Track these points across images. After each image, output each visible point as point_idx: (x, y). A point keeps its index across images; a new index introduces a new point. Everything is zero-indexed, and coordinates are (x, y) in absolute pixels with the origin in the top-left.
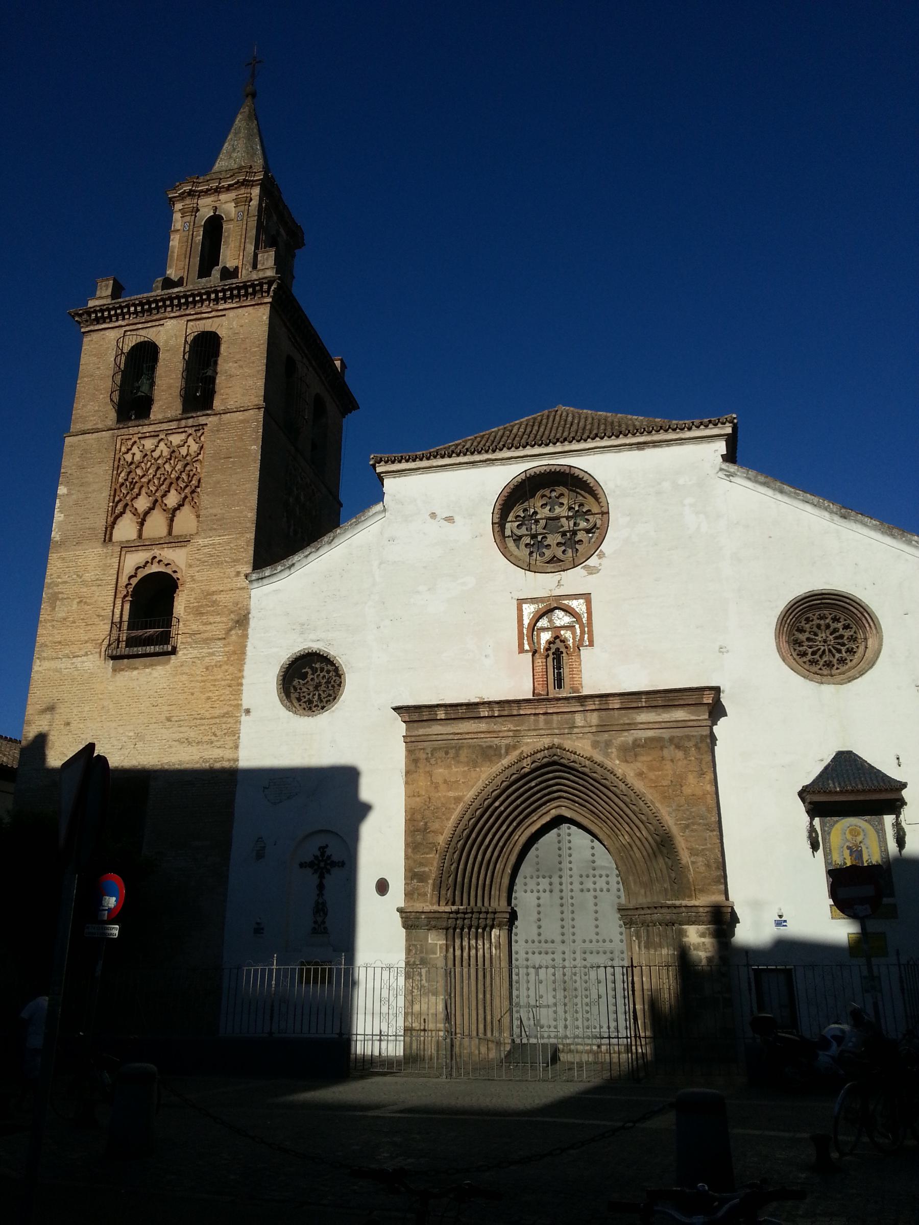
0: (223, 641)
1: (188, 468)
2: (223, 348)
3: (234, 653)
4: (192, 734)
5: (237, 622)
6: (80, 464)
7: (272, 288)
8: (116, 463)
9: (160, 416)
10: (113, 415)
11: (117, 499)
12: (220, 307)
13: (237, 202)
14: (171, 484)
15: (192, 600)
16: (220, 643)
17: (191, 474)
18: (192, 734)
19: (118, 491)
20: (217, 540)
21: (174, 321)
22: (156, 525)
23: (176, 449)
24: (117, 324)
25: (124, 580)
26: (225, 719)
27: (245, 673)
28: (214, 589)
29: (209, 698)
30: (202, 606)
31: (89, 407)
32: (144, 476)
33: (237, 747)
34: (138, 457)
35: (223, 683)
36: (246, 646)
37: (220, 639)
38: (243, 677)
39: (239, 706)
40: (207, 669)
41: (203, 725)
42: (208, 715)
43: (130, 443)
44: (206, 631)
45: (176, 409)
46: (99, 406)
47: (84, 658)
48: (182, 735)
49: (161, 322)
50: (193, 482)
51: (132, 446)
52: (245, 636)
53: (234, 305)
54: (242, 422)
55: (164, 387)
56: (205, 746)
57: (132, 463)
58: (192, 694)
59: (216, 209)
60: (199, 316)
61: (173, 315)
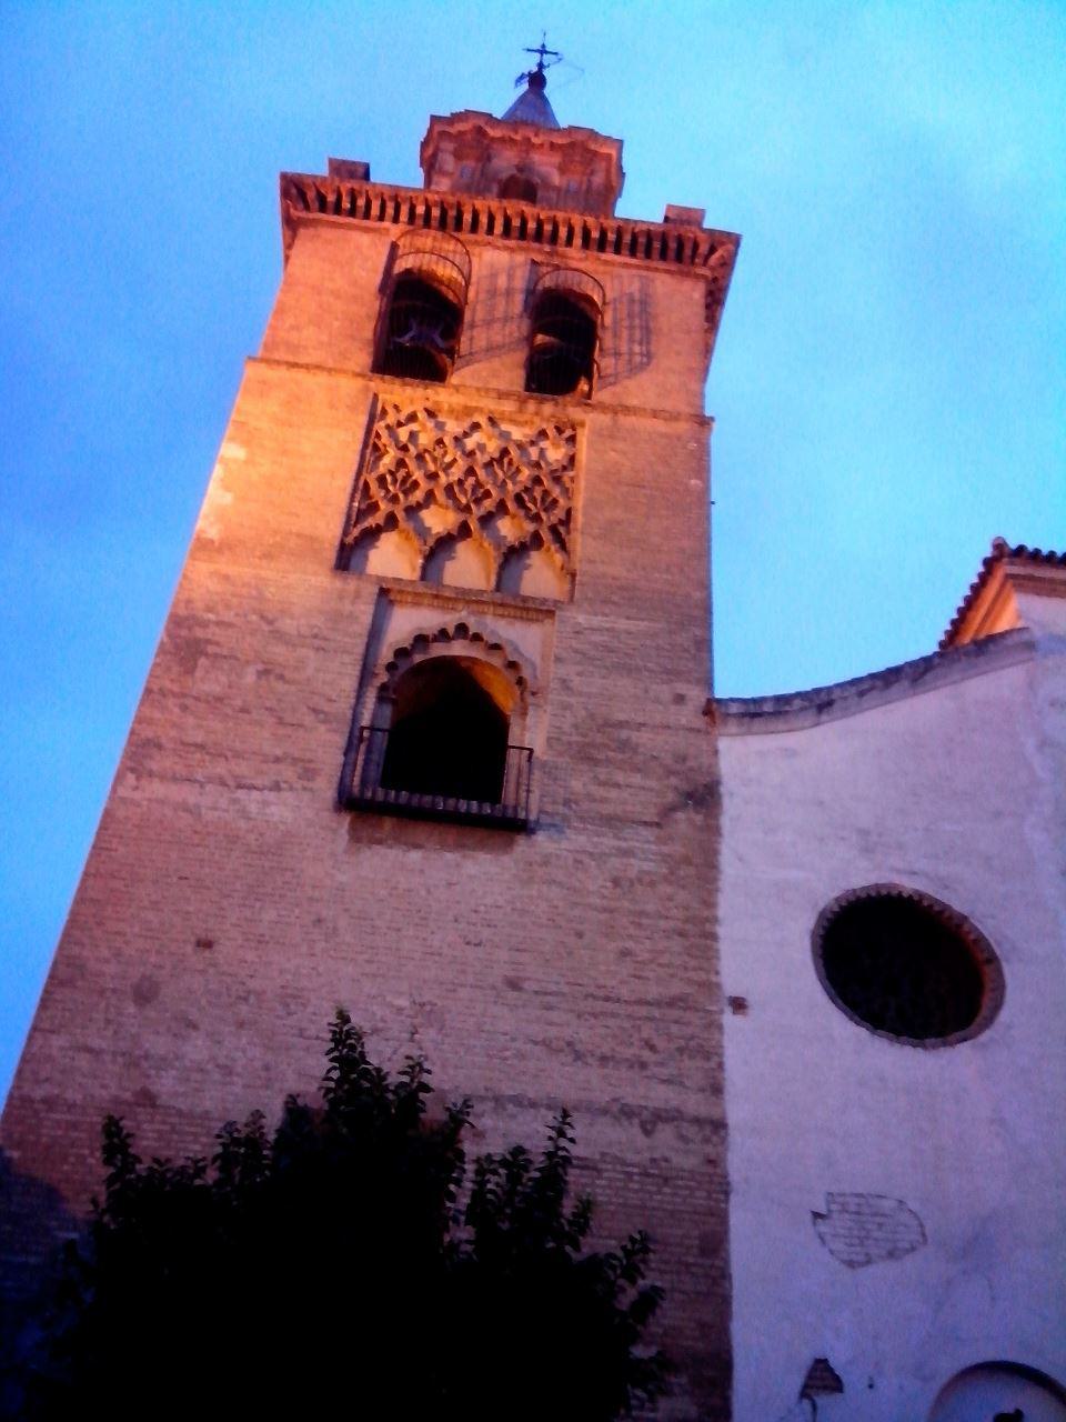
0: (656, 831)
3: (687, 861)
4: (584, 1034)
5: (690, 795)
15: (566, 728)
16: (646, 833)
18: (584, 1034)
20: (623, 624)
22: (468, 568)
25: (386, 655)
26: (675, 1013)
27: (722, 912)
28: (622, 717)
29: (625, 953)
30: (592, 745)
33: (717, 1089)
35: (662, 924)
36: (716, 853)
37: (645, 823)
38: (715, 920)
39: (711, 988)
40: (616, 882)
41: (614, 1015)
42: (624, 992)
44: (603, 800)
47: (271, 796)
48: (553, 1032)
52: (712, 830)
56: (624, 1072)
58: (580, 935)
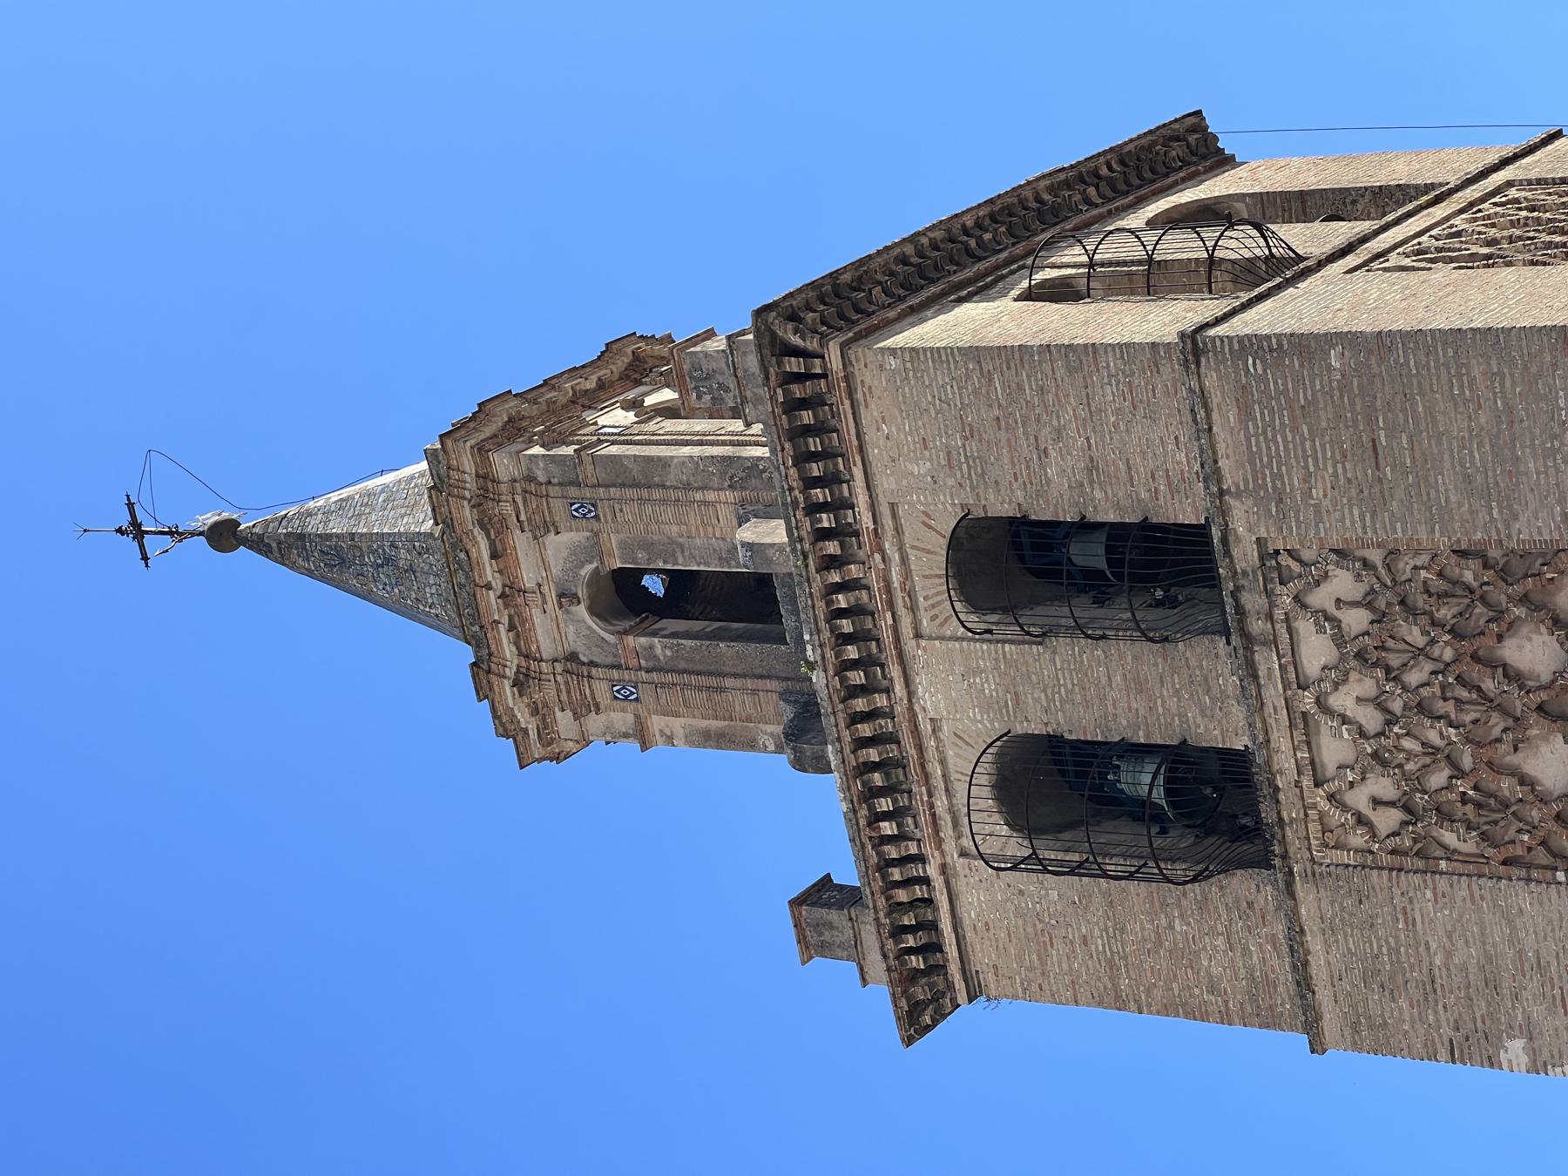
1: (1420, 601)
2: (1001, 506)
6: (1417, 995)
7: (796, 340)
8: (1408, 862)
9: (1238, 714)
10: (1241, 884)
11: (1541, 856)
12: (866, 521)
13: (543, 527)
14: (1475, 657)
17: (1441, 585)
19: (1511, 851)
21: (922, 682)
23: (1351, 649)
24: (938, 882)
31: (1216, 970)
32: (1452, 761)
34: (1382, 786)
43: (1336, 817)
45: (1210, 658)
46: (1213, 932)
49: (925, 727)
50: (1468, 576)
51: (1344, 807)
53: (858, 472)
54: (1246, 412)
55: (1139, 704)
57: (1408, 809)
59: (566, 597)
60: (899, 598)
61: (899, 689)
